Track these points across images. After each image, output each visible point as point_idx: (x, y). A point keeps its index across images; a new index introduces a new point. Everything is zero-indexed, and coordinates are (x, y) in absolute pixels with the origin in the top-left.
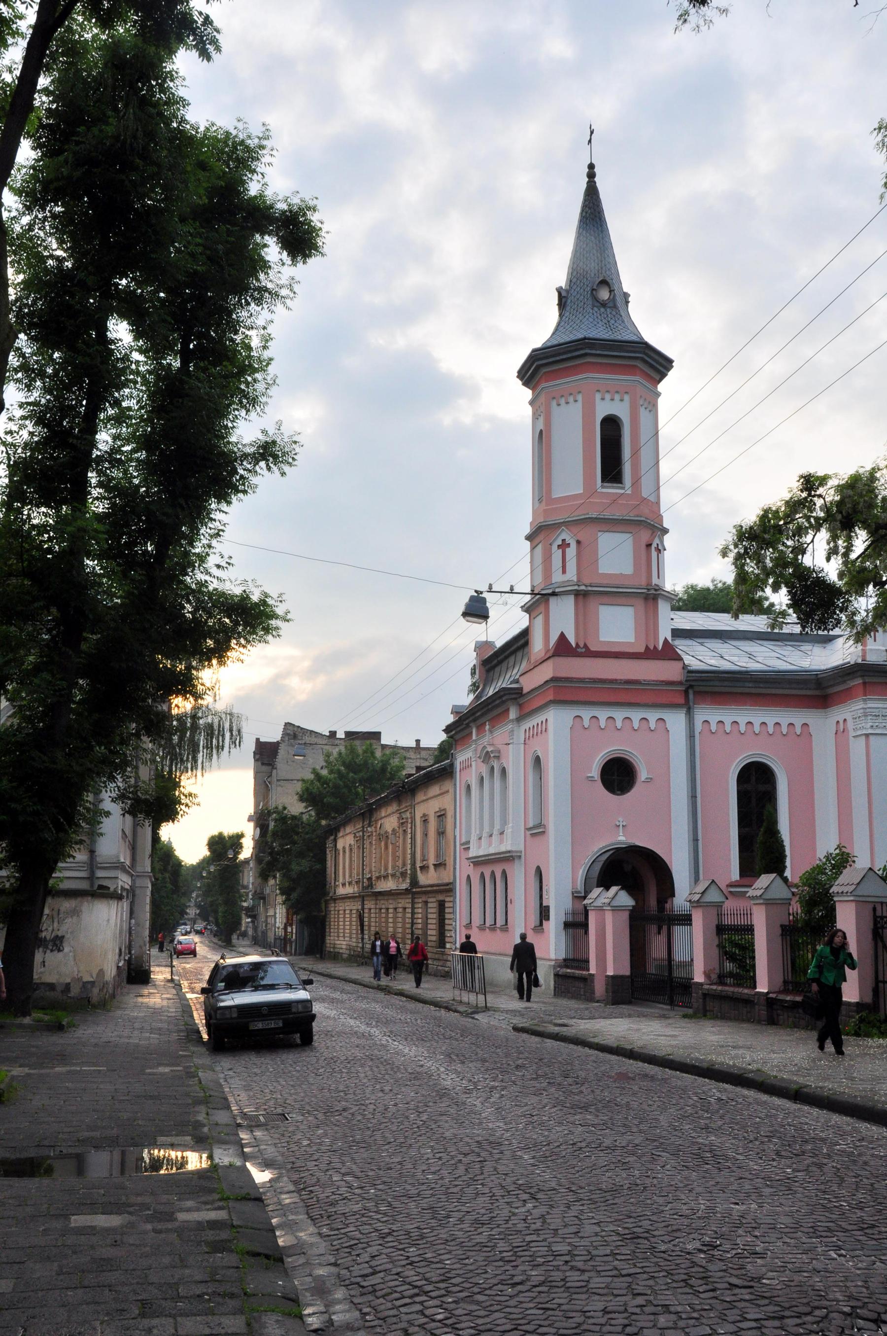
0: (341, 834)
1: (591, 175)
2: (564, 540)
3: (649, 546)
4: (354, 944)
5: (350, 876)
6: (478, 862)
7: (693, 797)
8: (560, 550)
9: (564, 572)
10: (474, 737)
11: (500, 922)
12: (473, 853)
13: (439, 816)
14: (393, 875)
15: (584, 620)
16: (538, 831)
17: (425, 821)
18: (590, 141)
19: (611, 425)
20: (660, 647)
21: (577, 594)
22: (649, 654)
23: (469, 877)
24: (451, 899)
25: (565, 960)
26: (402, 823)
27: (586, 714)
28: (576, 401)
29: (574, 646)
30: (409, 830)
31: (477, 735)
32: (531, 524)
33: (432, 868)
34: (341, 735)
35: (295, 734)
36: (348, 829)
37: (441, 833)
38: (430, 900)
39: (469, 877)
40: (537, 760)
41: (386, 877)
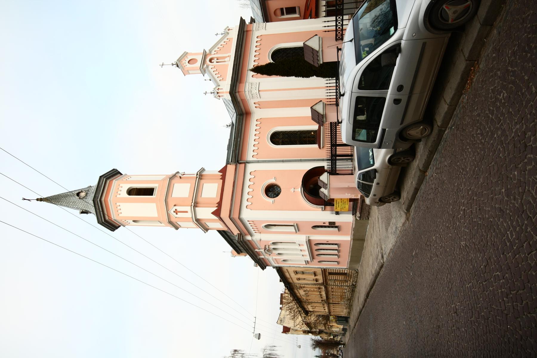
0: (308, 309)
1: (41, 200)
2: (174, 212)
3: (180, 177)
4: (345, 307)
5: (322, 307)
6: (313, 257)
7: (283, 161)
8: (178, 213)
9: (187, 212)
10: (263, 257)
11: (336, 247)
12: (309, 260)
13: (297, 273)
14: (320, 292)
15: (207, 205)
16: (297, 227)
17: (299, 279)
18: (29, 200)
19: (131, 192)
20: (221, 174)
21: (196, 205)
22: (223, 178)
23: (319, 262)
24: (328, 270)
25: (353, 215)
26: (301, 288)
27: (245, 203)
28: (120, 206)
29: (217, 208)
30: (303, 285)
31: (261, 255)
32: (171, 227)
33: (316, 277)
34: (281, 306)
35: (280, 321)
36: (306, 307)
37: (303, 273)
38: (328, 278)
39: (319, 262)
40: (268, 226)
41: (321, 295)
